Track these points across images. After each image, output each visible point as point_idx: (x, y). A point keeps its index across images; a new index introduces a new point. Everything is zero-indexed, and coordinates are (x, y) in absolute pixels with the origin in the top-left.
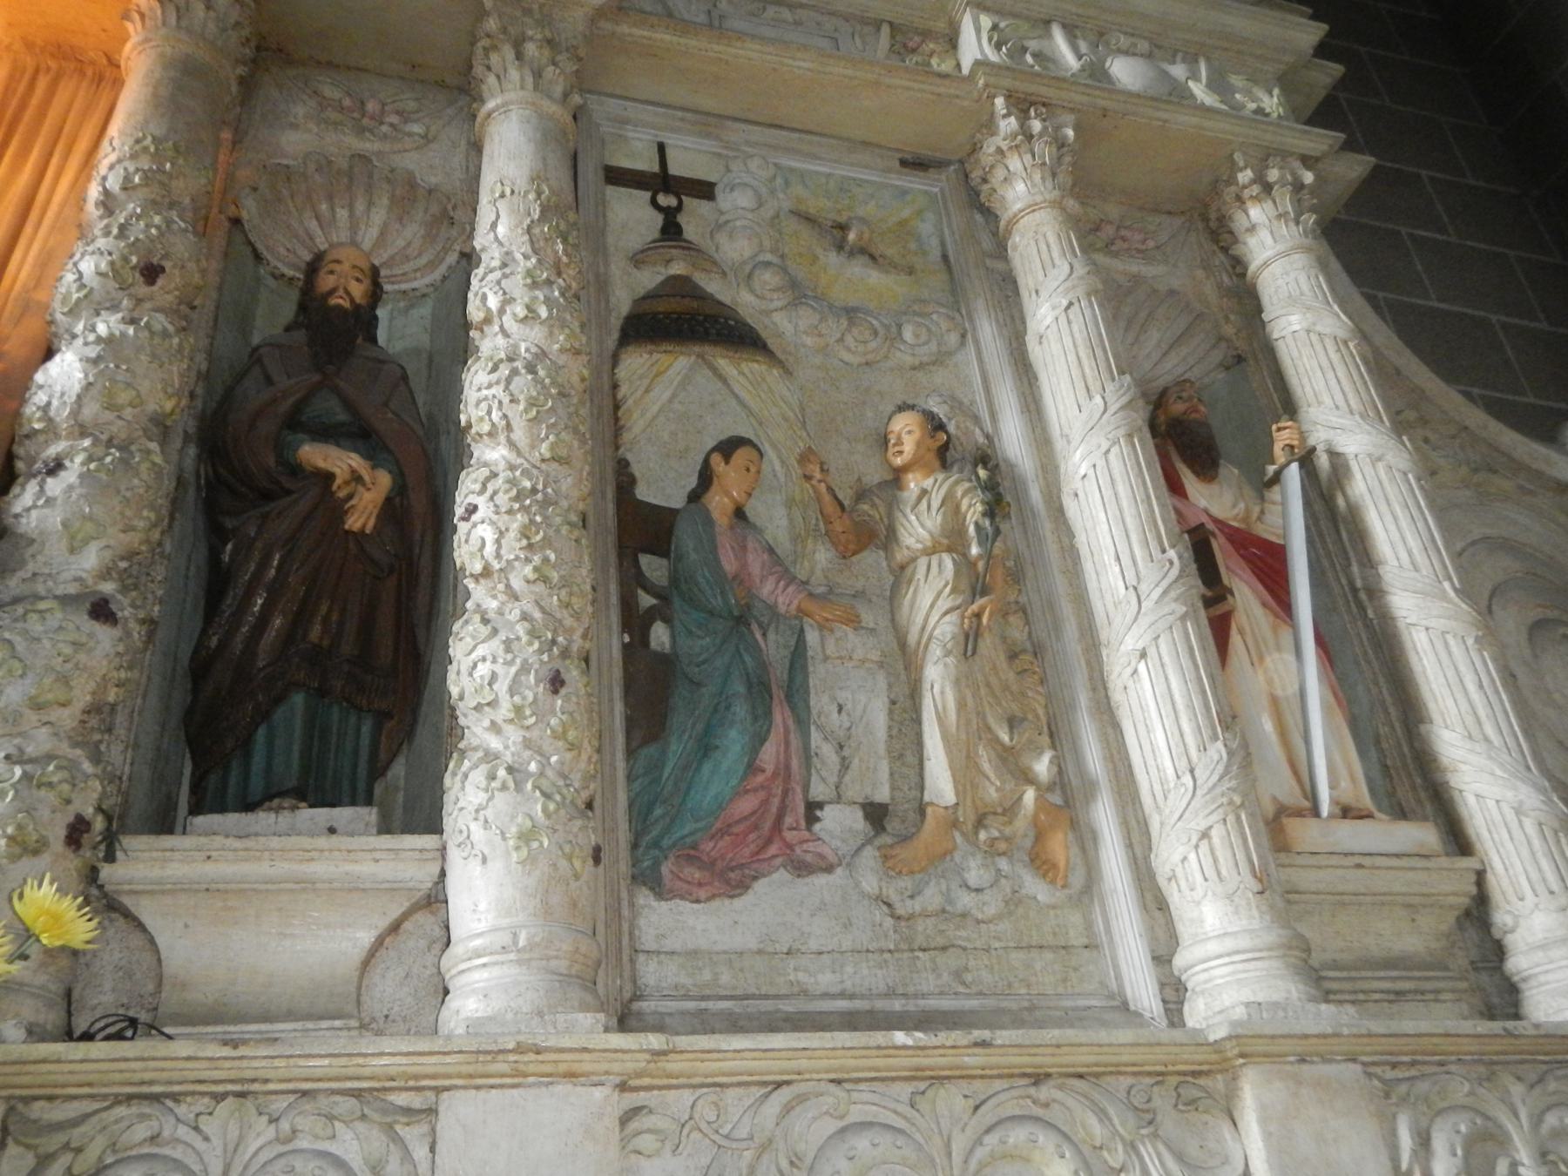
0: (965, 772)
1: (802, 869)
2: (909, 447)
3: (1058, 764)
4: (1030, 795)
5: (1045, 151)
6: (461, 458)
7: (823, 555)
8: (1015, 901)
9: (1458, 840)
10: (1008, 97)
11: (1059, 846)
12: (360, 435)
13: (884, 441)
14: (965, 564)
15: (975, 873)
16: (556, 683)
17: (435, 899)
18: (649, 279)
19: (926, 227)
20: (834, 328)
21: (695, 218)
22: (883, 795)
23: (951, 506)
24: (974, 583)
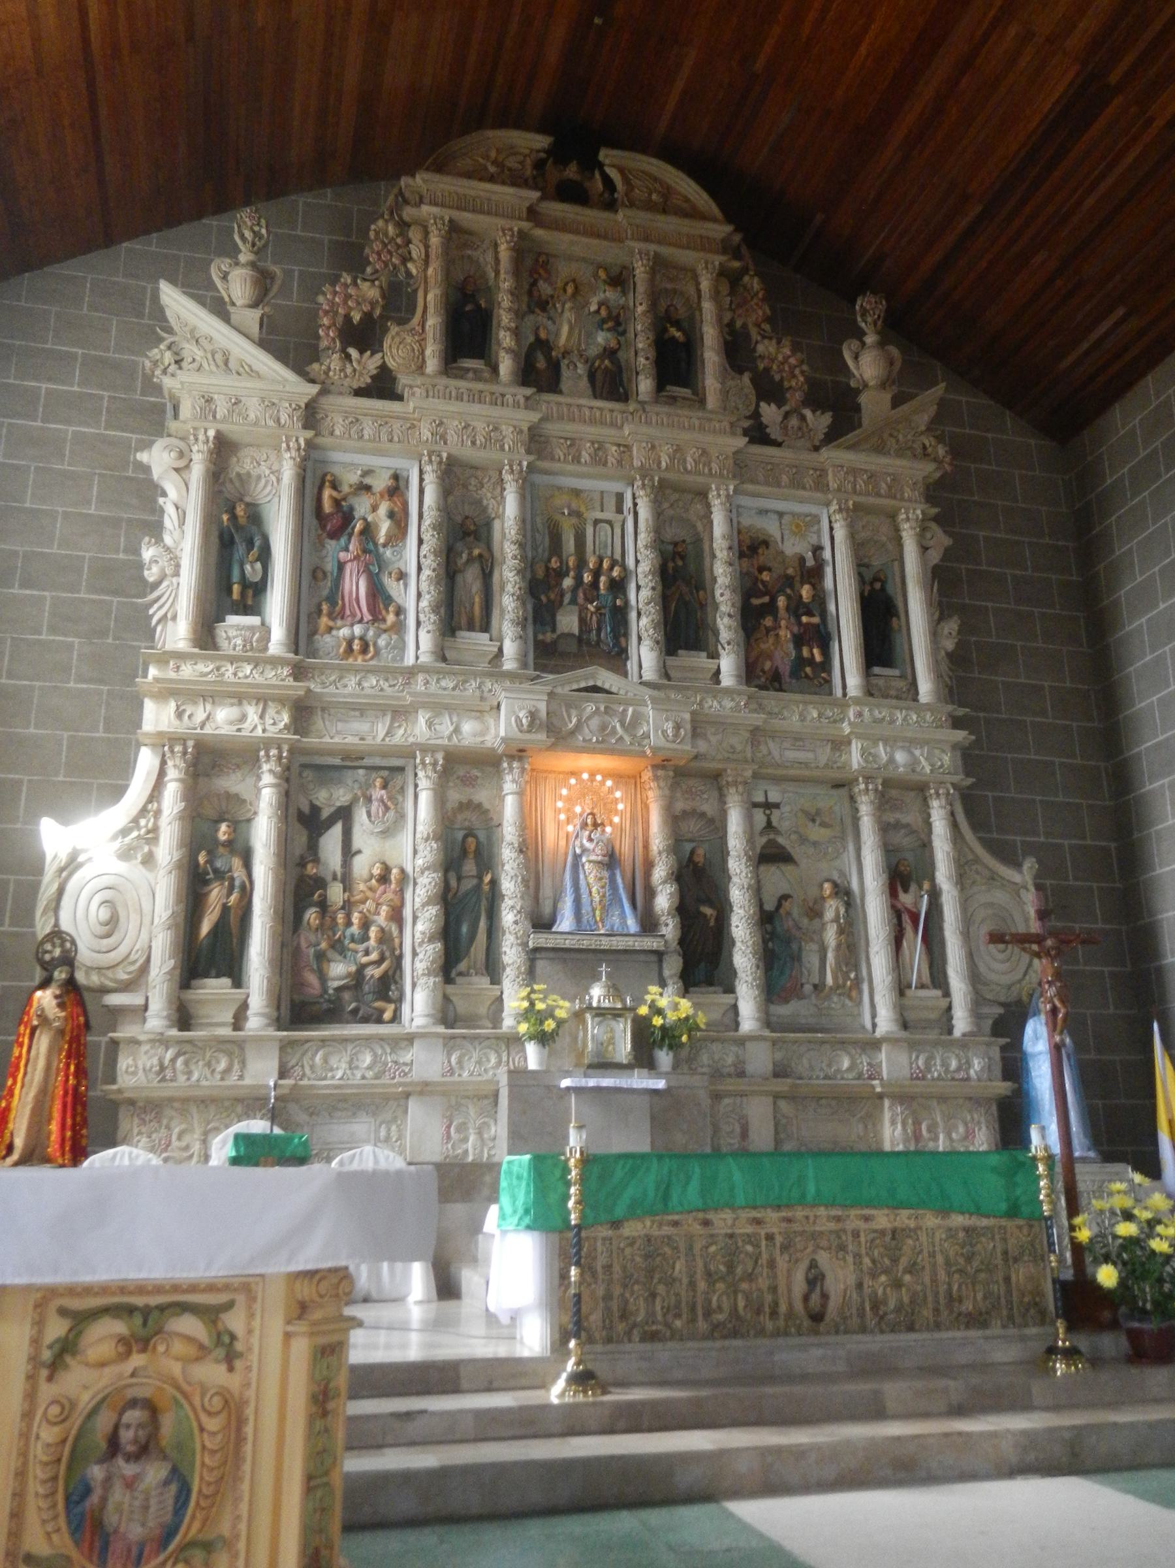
0: (835, 978)
1: (801, 997)
2: (828, 892)
3: (856, 975)
4: (849, 983)
5: (872, 795)
6: (732, 911)
7: (805, 921)
8: (843, 1006)
9: (947, 994)
10: (864, 777)
11: (854, 994)
12: (711, 904)
13: (821, 886)
14: (839, 925)
15: (835, 999)
16: (758, 967)
17: (735, 1008)
18: (764, 840)
19: (837, 808)
20: (811, 850)
21: (775, 816)
22: (817, 982)
23: (837, 911)
24: (841, 931)
